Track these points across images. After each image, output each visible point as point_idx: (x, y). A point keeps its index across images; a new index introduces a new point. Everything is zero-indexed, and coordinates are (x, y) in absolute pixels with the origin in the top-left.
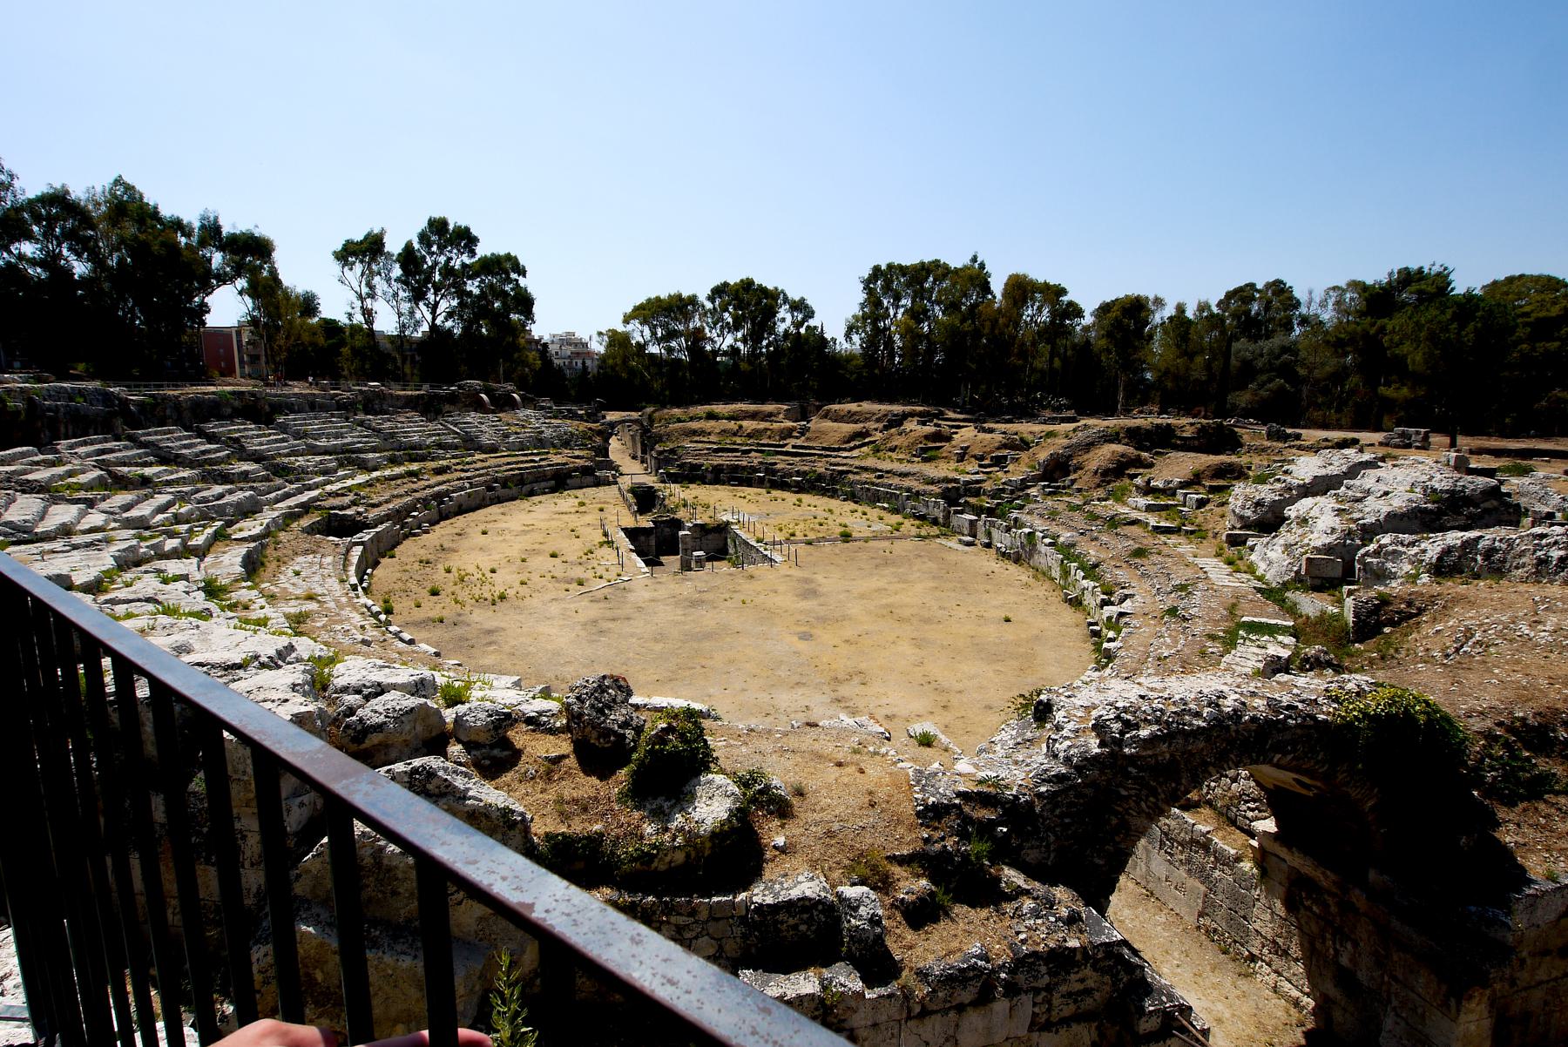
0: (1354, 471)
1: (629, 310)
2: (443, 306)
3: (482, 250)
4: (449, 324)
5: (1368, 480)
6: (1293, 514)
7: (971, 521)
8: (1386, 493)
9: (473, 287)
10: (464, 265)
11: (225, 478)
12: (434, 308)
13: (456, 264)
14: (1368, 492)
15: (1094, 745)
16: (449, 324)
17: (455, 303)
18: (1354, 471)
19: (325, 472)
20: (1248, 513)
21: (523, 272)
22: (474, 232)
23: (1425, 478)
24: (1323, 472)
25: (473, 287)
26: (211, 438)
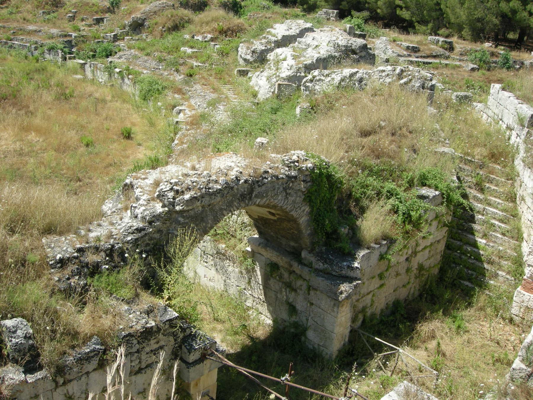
0: (302, 33)
5: (308, 38)
6: (272, 58)
8: (317, 46)
14: (309, 46)
15: (159, 208)
18: (302, 33)
20: (249, 57)
23: (334, 38)
24: (287, 33)
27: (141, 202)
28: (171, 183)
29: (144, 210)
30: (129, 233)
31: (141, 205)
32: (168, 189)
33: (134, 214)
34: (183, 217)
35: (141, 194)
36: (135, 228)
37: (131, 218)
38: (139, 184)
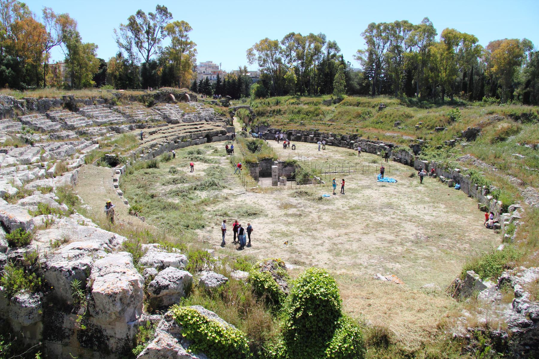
11: (59, 138)
19: (102, 135)
26: (53, 119)
29: (528, 307)
30: (515, 326)
31: (525, 302)
35: (522, 290)
36: (520, 322)
38: (517, 280)
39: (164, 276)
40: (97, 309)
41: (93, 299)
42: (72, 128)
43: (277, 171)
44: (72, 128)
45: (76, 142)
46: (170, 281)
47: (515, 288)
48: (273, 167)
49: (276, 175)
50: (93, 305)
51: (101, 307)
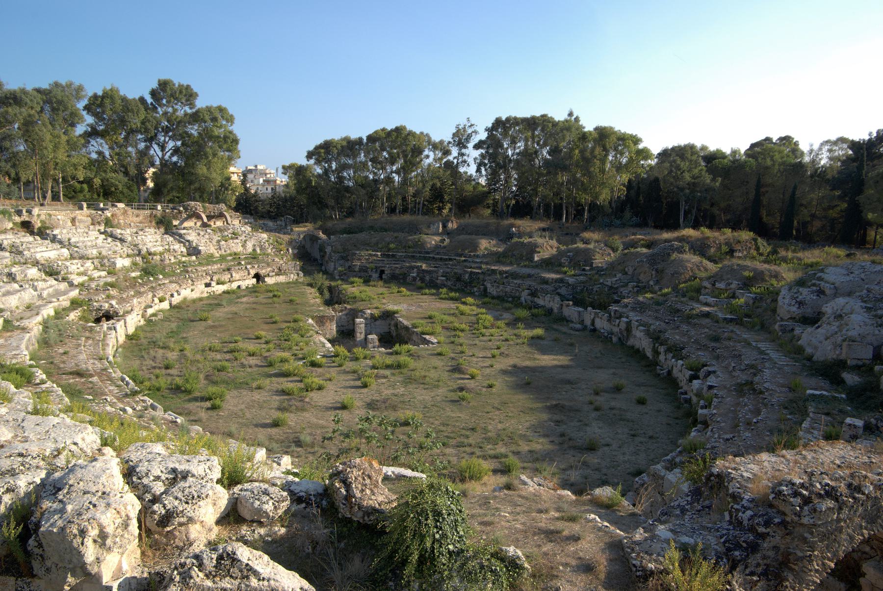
1: (311, 148)
2: (171, 144)
3: (201, 103)
4: (175, 159)
7: (579, 312)
9: (194, 130)
10: (186, 114)
12: (163, 148)
13: (180, 113)
16: (175, 159)
17: (179, 143)
21: (231, 119)
22: (195, 88)
25: (194, 130)
27: (744, 502)
28: (793, 484)
32: (790, 492)
33: (737, 519)
34: (812, 533)
37: (730, 523)
39: (176, 494)
40: (48, 563)
41: (40, 545)
42: (36, 263)
43: (363, 325)
44: (36, 263)
45: (40, 285)
46: (187, 503)
47: (730, 487)
48: (358, 320)
49: (361, 333)
50: (41, 556)
51: (55, 559)
